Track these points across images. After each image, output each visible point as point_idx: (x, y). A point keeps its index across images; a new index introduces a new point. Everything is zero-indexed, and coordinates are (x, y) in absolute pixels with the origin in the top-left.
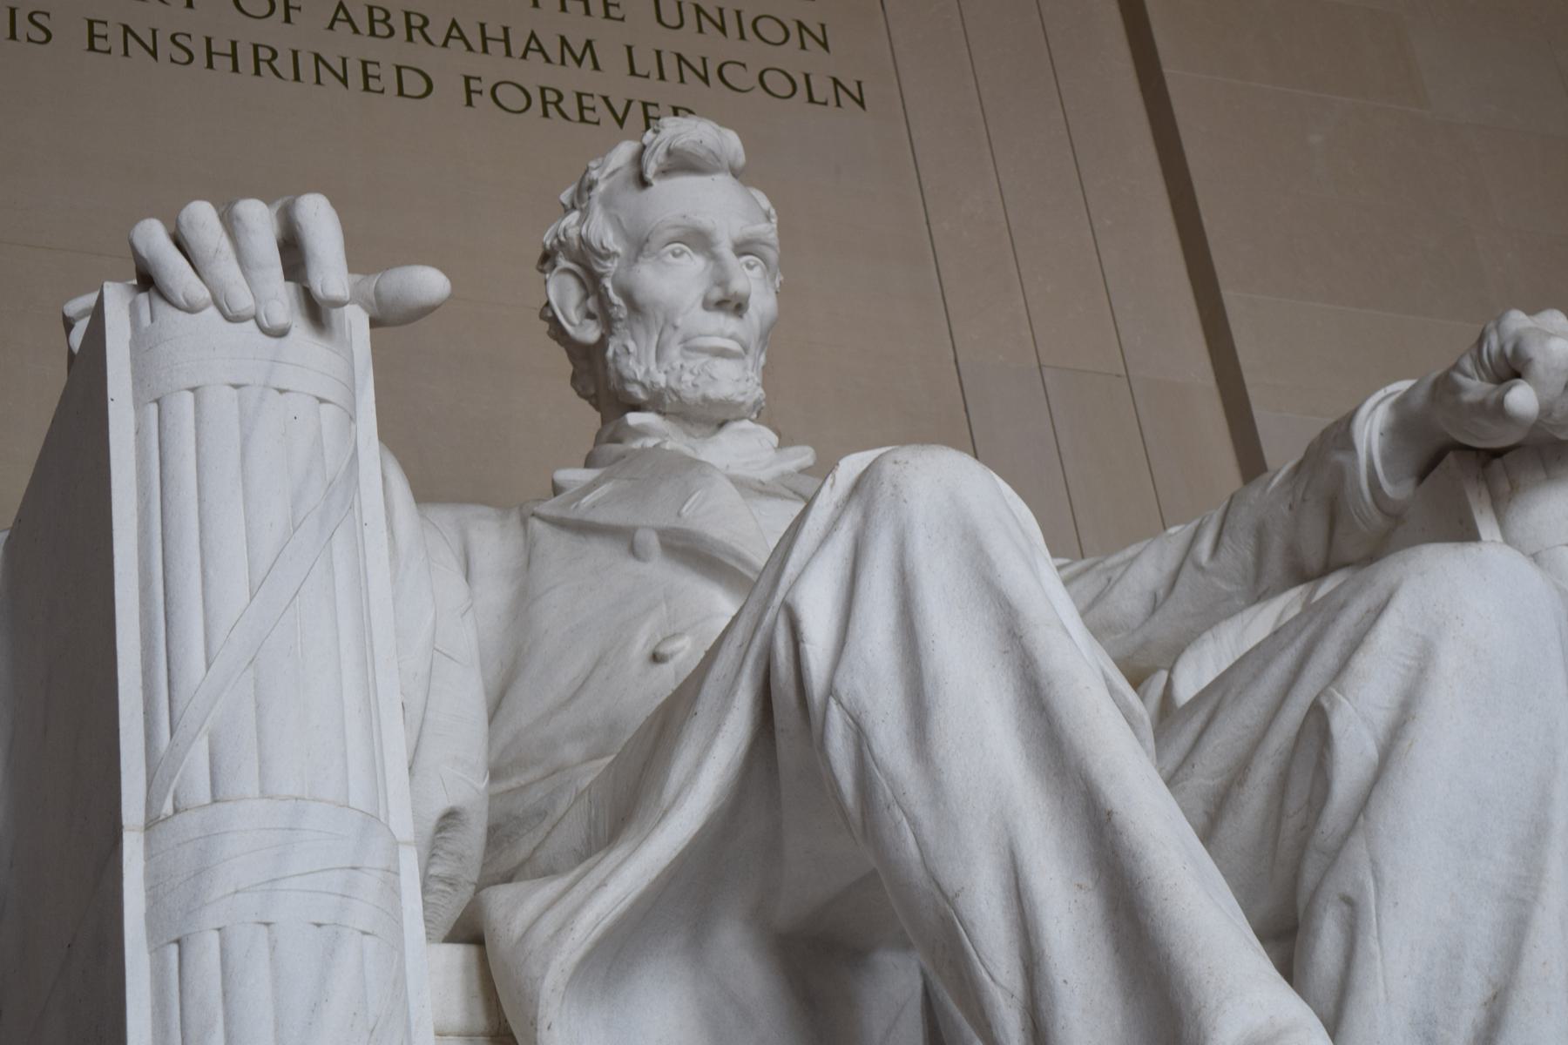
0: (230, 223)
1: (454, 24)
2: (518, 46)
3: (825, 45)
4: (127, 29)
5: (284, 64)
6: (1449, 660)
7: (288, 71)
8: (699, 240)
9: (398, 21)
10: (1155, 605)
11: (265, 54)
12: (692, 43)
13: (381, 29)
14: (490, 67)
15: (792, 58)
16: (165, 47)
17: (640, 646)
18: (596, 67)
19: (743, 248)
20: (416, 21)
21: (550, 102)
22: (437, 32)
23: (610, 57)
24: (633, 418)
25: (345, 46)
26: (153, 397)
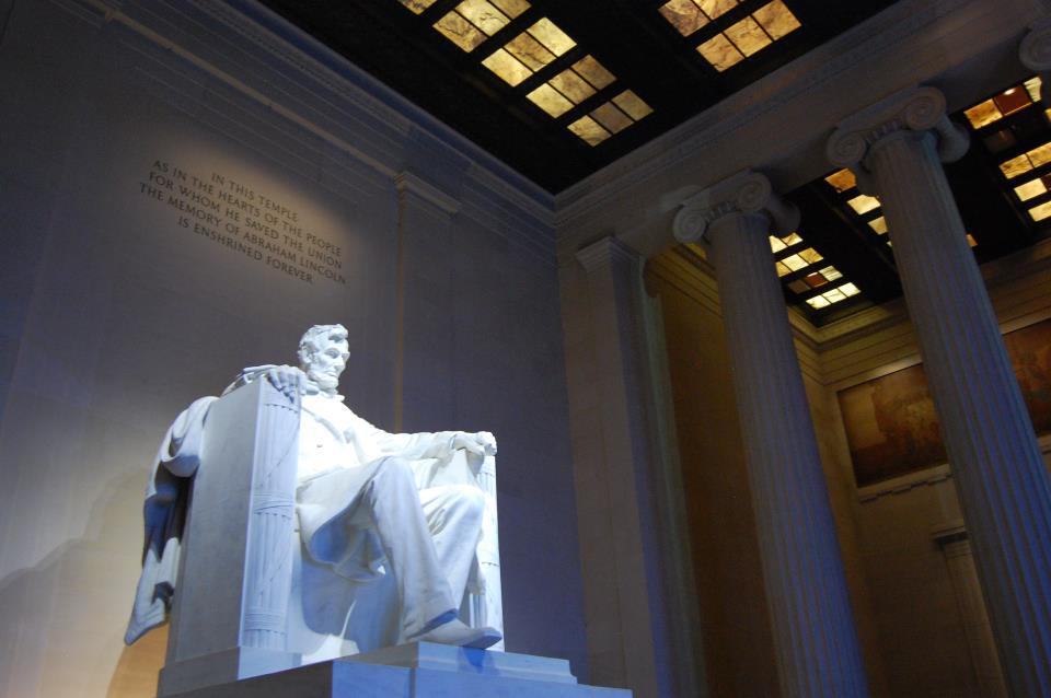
15: (332, 268)
22: (265, 244)
23: (298, 260)
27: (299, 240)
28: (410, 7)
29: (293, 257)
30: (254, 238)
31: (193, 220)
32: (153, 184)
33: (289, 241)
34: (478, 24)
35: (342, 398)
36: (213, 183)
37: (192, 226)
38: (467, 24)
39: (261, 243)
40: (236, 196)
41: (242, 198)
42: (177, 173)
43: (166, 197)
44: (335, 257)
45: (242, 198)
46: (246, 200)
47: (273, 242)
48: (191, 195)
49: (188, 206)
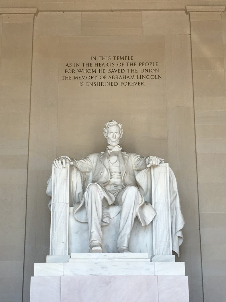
0: (58, 162)
1: (121, 76)
2: (126, 78)
3: (158, 71)
4: (90, 83)
6: (127, 195)
7: (104, 85)
10: (141, 165)
11: (102, 83)
12: (144, 74)
13: (113, 78)
14: (124, 81)
15: (154, 74)
16: (94, 84)
17: (100, 172)
18: (134, 79)
19: (115, 133)
20: (117, 77)
21: (129, 84)
22: (119, 78)
23: (136, 77)
24: (108, 146)
25: (110, 81)
26: (55, 173)
30: (113, 77)
31: (85, 81)
32: (67, 74)
33: (130, 71)
35: (121, 148)
37: (85, 84)
39: (117, 77)
41: (105, 62)
42: (76, 64)
43: (73, 77)
44: (155, 68)
45: (105, 62)
46: (108, 61)
48: (83, 72)
49: (82, 76)
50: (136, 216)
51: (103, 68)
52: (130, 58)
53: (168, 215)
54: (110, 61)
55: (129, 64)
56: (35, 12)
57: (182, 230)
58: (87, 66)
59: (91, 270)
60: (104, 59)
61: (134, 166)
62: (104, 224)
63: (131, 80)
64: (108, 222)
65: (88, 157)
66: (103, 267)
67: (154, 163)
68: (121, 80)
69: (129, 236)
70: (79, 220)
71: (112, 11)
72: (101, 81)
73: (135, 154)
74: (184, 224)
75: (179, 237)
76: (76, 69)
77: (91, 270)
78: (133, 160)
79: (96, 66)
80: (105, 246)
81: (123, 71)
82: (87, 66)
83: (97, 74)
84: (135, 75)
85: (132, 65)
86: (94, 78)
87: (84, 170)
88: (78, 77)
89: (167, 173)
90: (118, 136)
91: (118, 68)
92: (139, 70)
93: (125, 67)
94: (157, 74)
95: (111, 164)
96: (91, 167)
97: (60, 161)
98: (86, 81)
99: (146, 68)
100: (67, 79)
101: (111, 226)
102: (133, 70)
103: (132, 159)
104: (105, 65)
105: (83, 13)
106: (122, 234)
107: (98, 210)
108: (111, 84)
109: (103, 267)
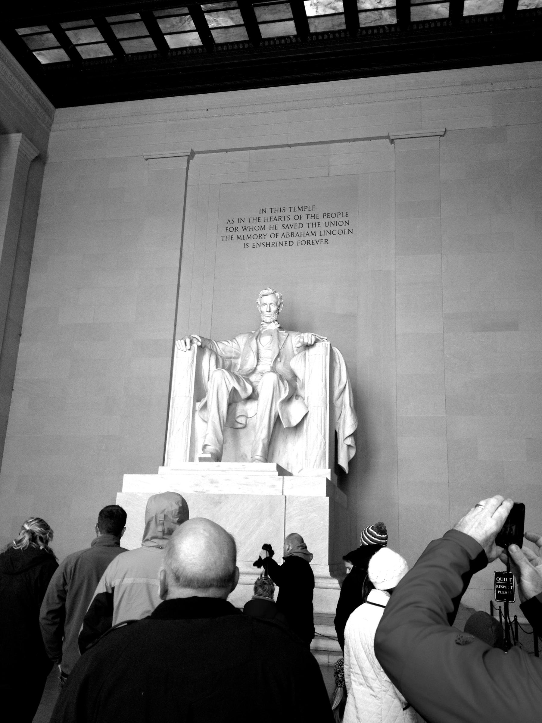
5: (275, 245)
8: (266, 304)
9: (290, 235)
15: (343, 228)
16: (261, 245)
21: (308, 242)
22: (295, 235)
23: (318, 234)
25: (283, 240)
27: (317, 221)
28: (338, 28)
29: (314, 234)
30: (288, 234)
31: (250, 242)
32: (229, 234)
33: (311, 225)
34: (381, 6)
35: (279, 326)
36: (260, 215)
37: (250, 245)
38: (376, 12)
39: (292, 234)
40: (274, 215)
41: (277, 215)
42: (240, 220)
43: (235, 237)
44: (344, 219)
45: (277, 215)
47: (299, 231)
50: (277, 414)
51: (275, 223)
52: (311, 208)
53: (325, 414)
54: (284, 214)
55: (309, 216)
56: (189, 154)
57: (354, 435)
58: (255, 221)
59: (197, 485)
60: (276, 211)
61: (295, 349)
62: (239, 426)
63: (311, 238)
64: (244, 422)
65: (237, 339)
66: (212, 482)
67: (306, 341)
68: (298, 238)
69: (266, 441)
70: (206, 420)
71: (289, 146)
72: (271, 240)
73: (297, 333)
74: (355, 428)
75: (349, 446)
76: (240, 226)
77: (197, 485)
78: (295, 340)
79: (266, 220)
80: (242, 456)
81: (301, 226)
82: (255, 221)
83: (268, 232)
84: (317, 230)
85: (313, 218)
86: (263, 236)
87: (228, 355)
88: (242, 236)
89: (326, 355)
90: (274, 308)
91: (295, 222)
92: (322, 225)
93: (304, 221)
94: (347, 227)
95: (260, 347)
96: (238, 351)
97: (183, 341)
98: (253, 241)
99: (332, 220)
100: (228, 239)
101: (249, 428)
102: (314, 224)
103: (292, 339)
104: (278, 219)
105: (252, 151)
106: (257, 438)
107: (220, 405)
108: (284, 245)
109: (212, 482)
